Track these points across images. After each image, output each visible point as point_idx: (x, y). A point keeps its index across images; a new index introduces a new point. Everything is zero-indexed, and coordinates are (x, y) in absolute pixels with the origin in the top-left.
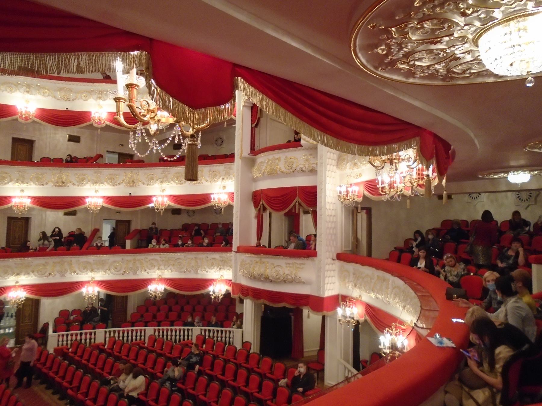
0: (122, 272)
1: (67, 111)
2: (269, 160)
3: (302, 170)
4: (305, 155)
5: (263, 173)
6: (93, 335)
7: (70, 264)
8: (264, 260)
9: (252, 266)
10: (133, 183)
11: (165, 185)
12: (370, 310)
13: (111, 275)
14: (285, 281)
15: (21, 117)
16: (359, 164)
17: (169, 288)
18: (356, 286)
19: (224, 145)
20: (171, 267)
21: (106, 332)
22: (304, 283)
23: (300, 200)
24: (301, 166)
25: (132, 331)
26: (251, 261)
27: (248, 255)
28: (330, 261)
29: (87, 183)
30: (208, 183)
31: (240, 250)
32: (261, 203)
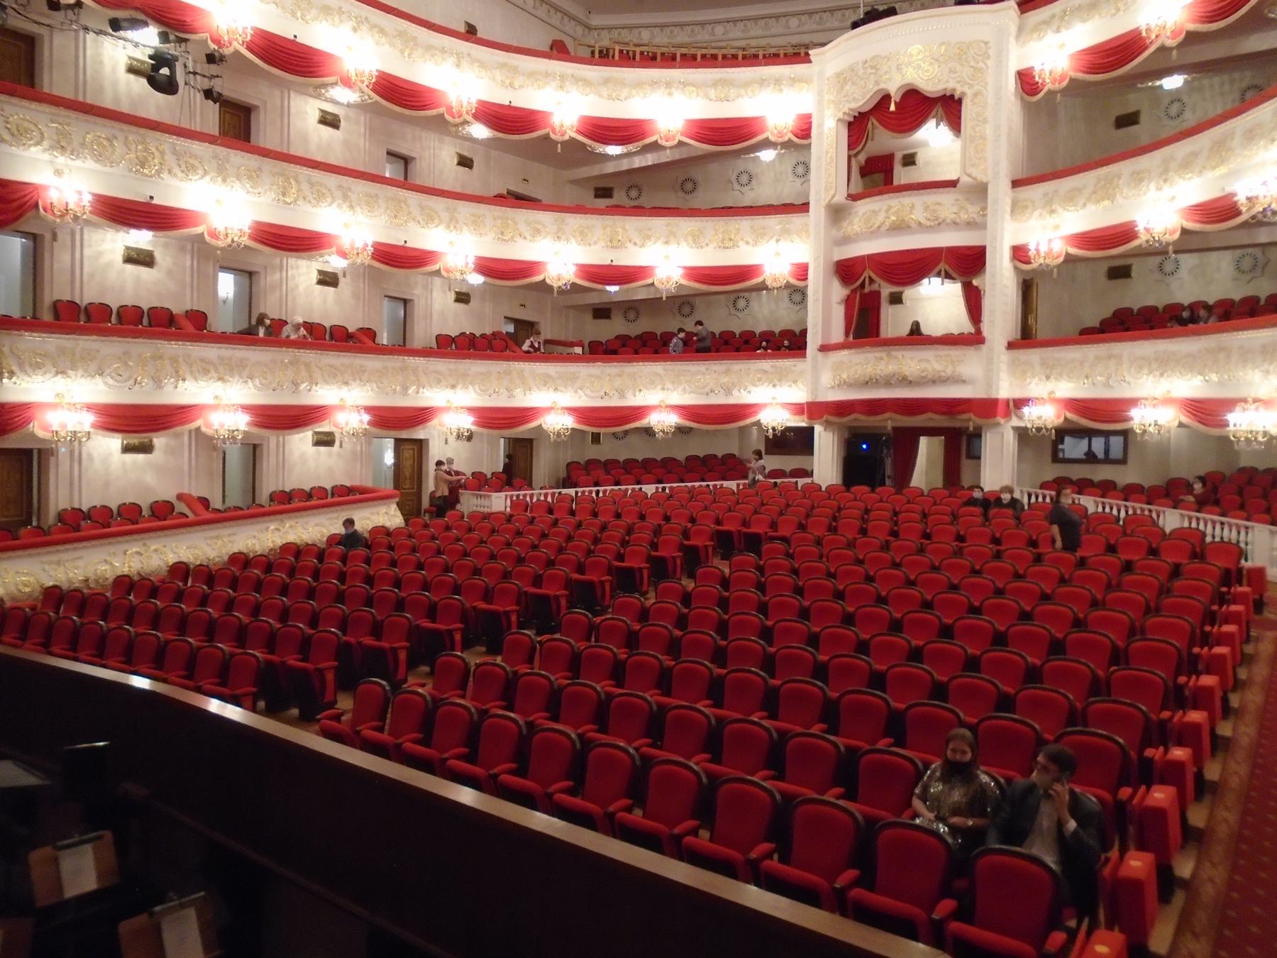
1: (509, 107)
2: (890, 208)
3: (955, 223)
7: (521, 375)
8: (894, 353)
10: (614, 243)
11: (673, 247)
13: (584, 397)
14: (934, 382)
15: (450, 109)
18: (1048, 378)
22: (964, 382)
23: (947, 268)
24: (953, 216)
27: (845, 352)
28: (1003, 349)
31: (825, 348)
32: (866, 274)
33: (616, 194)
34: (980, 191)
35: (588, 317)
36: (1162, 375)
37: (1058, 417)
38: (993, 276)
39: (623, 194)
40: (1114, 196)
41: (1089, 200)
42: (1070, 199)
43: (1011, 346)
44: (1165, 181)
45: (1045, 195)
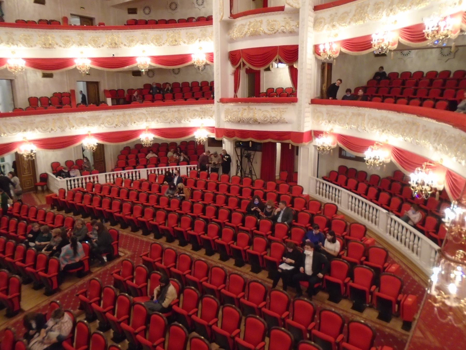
0: (114, 125)
2: (250, 23)
3: (283, 32)
4: (285, 18)
5: (245, 34)
6: (96, 179)
7: (68, 120)
8: (251, 107)
9: (240, 113)
10: (115, 45)
12: (342, 138)
13: (105, 128)
14: (271, 123)
16: (337, 25)
17: (156, 137)
18: (329, 122)
19: (179, 10)
20: (157, 119)
21: (106, 175)
23: (280, 58)
24: (283, 28)
25: (136, 172)
26: (238, 109)
27: (232, 104)
28: (307, 105)
29: (72, 45)
30: (186, 45)
31: (222, 101)
32: (241, 61)
33: (138, 12)
34: (296, 13)
35: (131, 76)
36: (383, 131)
37: (334, 144)
38: (302, 64)
39: (142, 12)
40: (365, 18)
41: (352, 20)
42: (342, 19)
43: (313, 102)
44: (391, 10)
45: (331, 15)
